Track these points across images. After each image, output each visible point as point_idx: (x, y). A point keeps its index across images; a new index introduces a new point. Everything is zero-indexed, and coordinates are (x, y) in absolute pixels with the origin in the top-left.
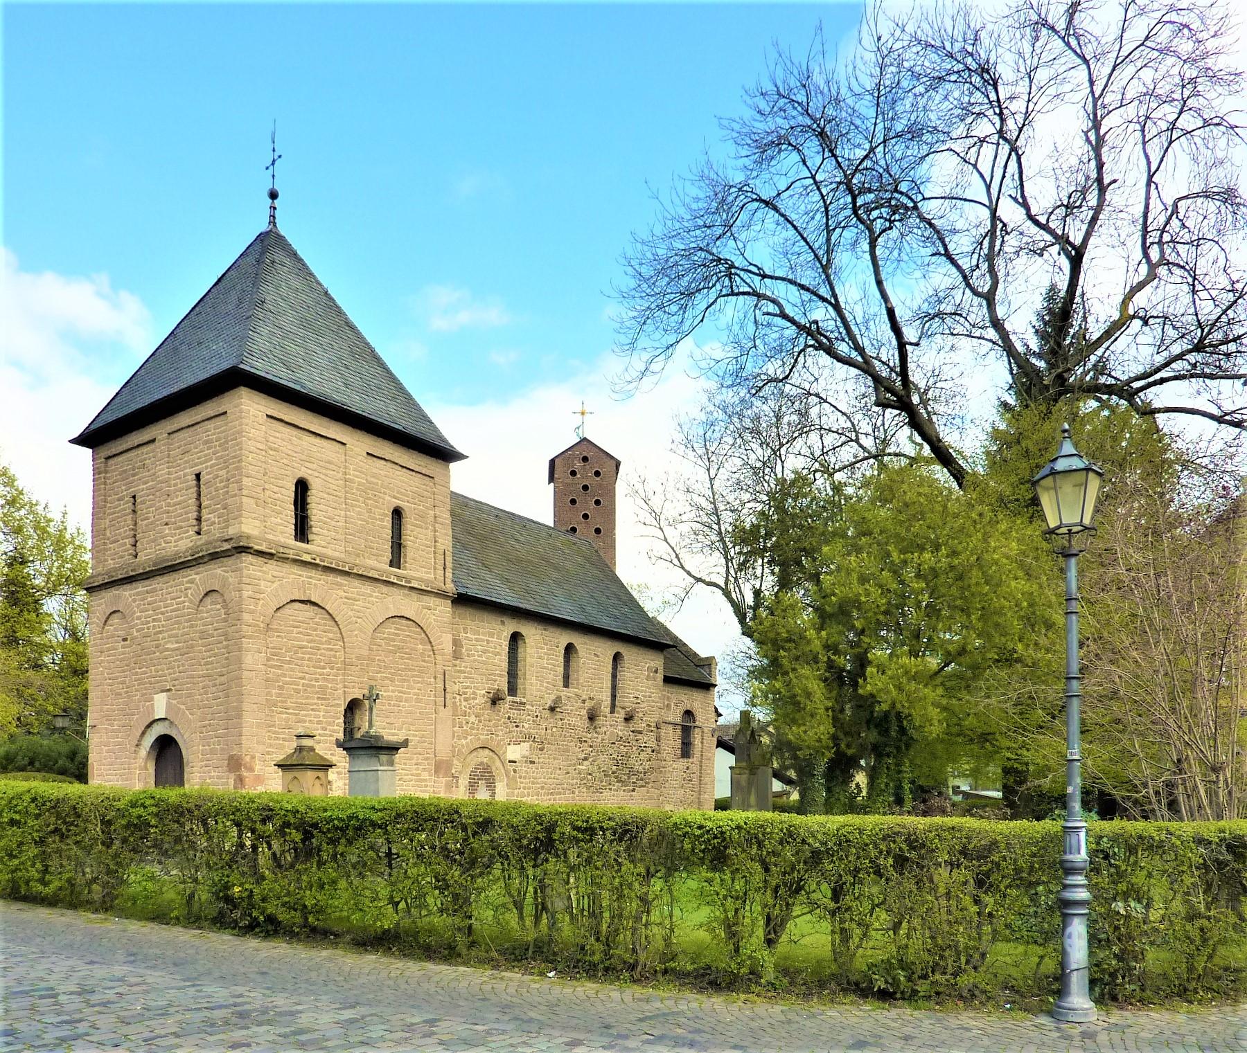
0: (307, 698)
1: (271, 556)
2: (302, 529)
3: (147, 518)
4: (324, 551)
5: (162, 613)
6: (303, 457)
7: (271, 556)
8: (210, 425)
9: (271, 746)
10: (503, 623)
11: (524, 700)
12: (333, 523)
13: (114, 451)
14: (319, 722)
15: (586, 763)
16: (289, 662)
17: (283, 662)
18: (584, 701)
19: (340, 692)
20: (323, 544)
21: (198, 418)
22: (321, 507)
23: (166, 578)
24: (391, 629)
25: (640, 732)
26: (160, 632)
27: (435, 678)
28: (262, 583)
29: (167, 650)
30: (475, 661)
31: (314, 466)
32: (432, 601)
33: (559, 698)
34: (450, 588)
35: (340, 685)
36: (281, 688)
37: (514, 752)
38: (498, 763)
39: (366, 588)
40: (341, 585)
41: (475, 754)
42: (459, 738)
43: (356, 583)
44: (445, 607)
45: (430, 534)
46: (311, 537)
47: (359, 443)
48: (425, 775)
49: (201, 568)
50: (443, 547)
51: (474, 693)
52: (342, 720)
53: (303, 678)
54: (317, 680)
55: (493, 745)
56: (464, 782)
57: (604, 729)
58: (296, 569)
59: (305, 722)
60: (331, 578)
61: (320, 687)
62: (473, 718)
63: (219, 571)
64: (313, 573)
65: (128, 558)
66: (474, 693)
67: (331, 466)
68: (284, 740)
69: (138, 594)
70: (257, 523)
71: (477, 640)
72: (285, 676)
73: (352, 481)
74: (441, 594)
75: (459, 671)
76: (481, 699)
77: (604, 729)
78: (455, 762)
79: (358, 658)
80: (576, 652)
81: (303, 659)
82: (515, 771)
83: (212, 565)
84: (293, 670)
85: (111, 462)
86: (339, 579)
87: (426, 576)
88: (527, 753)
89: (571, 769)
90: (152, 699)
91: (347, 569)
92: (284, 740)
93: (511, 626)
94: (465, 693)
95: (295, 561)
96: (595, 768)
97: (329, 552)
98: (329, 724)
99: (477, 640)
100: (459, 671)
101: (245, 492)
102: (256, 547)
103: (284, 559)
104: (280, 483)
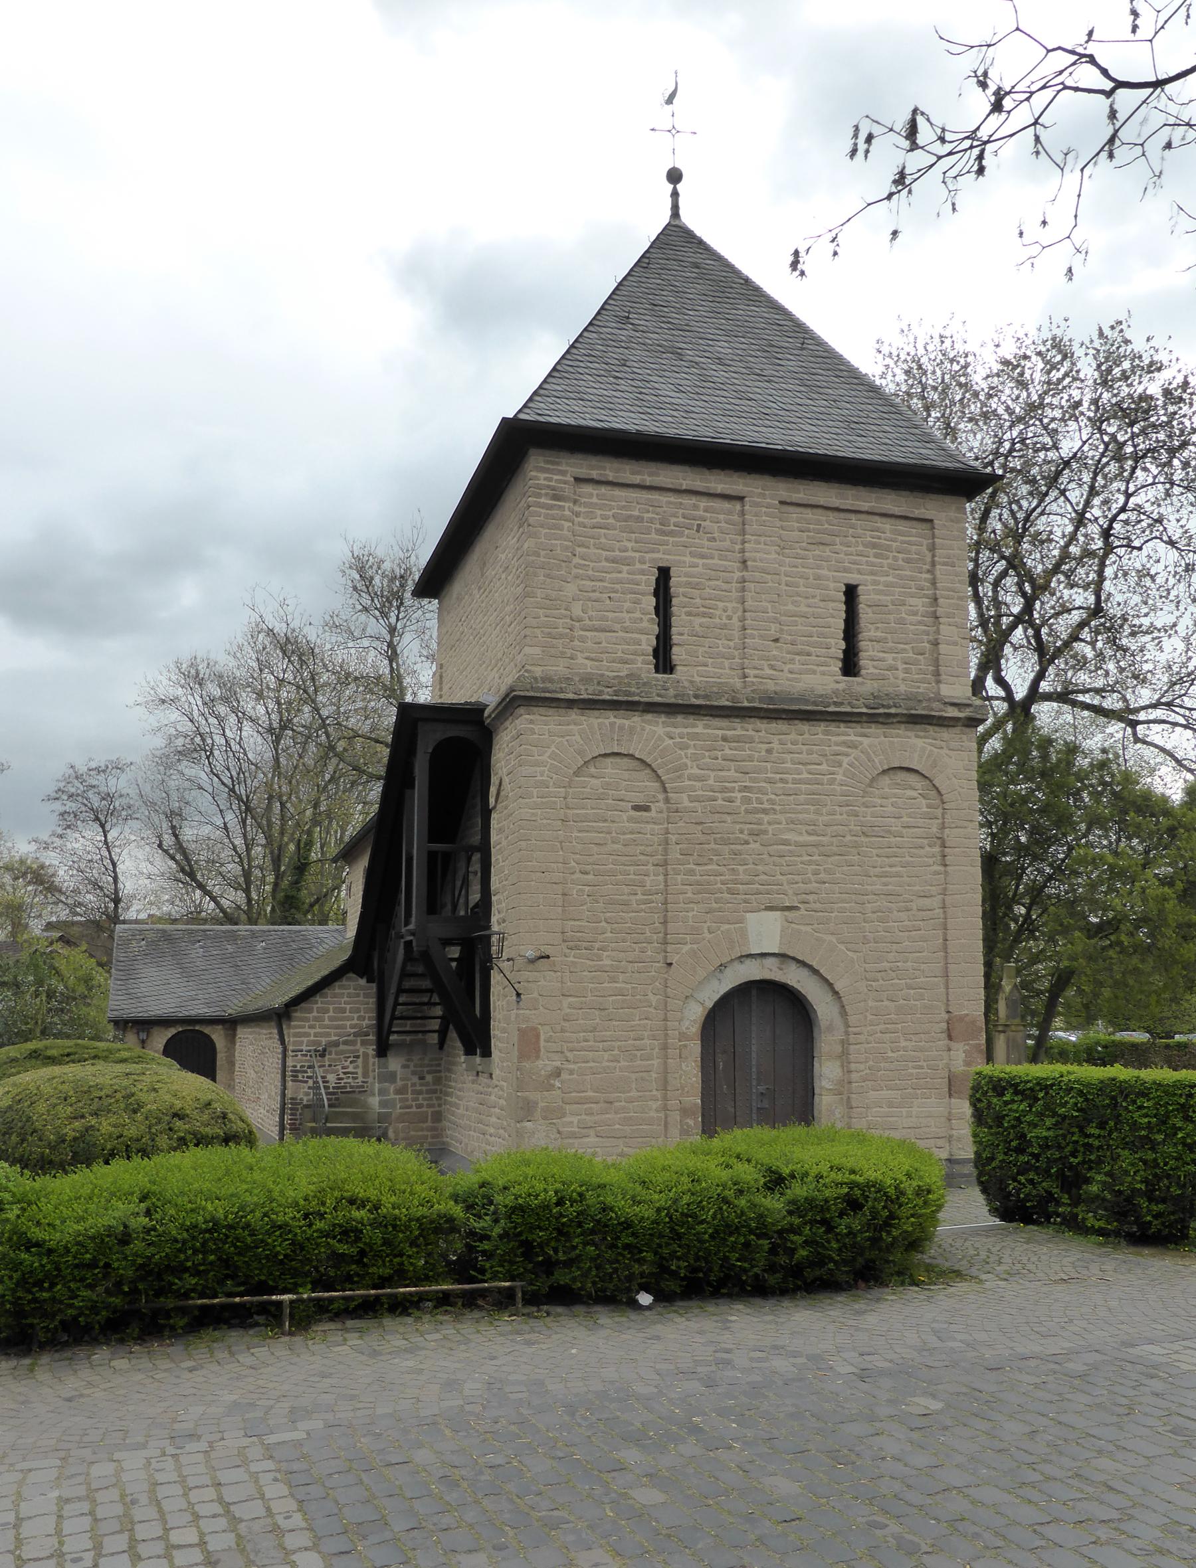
3: (704, 615)
5: (771, 782)
8: (887, 525)
13: (594, 474)
21: (865, 506)
23: (781, 726)
26: (765, 811)
29: (786, 843)
49: (873, 729)
63: (920, 742)
65: (644, 665)
69: (694, 737)
83: (901, 730)
85: (588, 489)
90: (741, 921)
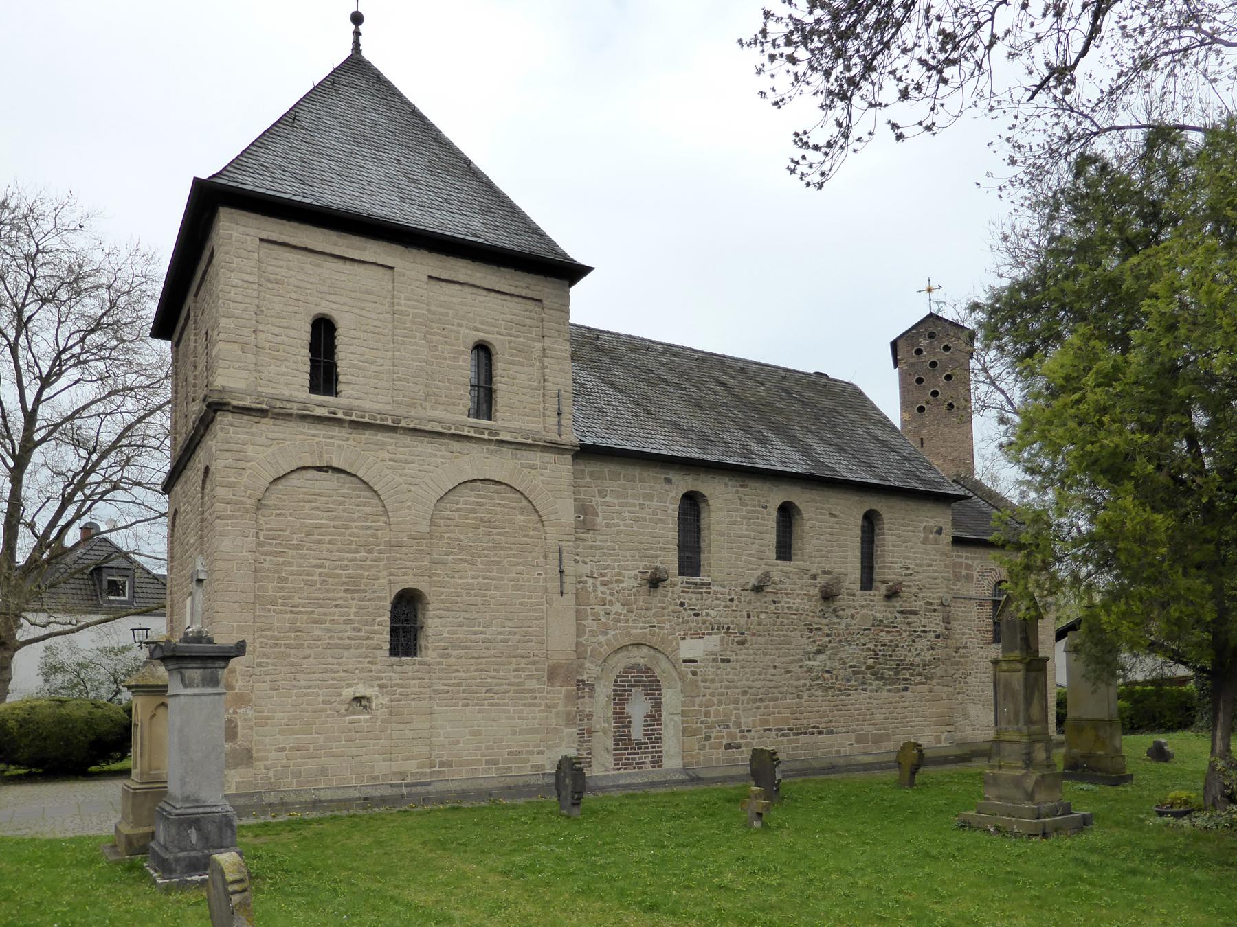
0: (327, 591)
1: (263, 413)
2: (324, 375)
4: (356, 403)
6: (326, 289)
7: (263, 413)
9: (265, 655)
10: (668, 481)
11: (706, 580)
12: (374, 368)
14: (347, 622)
15: (820, 657)
16: (297, 547)
17: (286, 547)
18: (814, 577)
19: (385, 581)
20: (356, 394)
22: (351, 349)
24: (469, 497)
25: (914, 613)
27: (545, 557)
28: (250, 448)
30: (619, 532)
31: (343, 299)
32: (537, 458)
33: (766, 575)
34: (571, 437)
35: (385, 573)
36: (285, 580)
37: (690, 648)
38: (665, 664)
39: (425, 446)
40: (383, 444)
41: (623, 653)
42: (593, 633)
43: (408, 440)
44: (563, 467)
45: (535, 372)
46: (340, 387)
47: (415, 267)
48: (532, 684)
50: (557, 387)
51: (619, 574)
52: (387, 618)
53: (321, 566)
54: (343, 568)
55: (653, 641)
56: (604, 690)
57: (848, 612)
58: (307, 428)
59: (325, 622)
60: (367, 435)
61: (349, 576)
62: (617, 608)
64: (336, 431)
66: (619, 574)
67: (367, 297)
68: (288, 646)
70: (244, 374)
71: (621, 505)
72: (290, 564)
73: (402, 313)
74: (555, 448)
75: (591, 547)
76: (631, 581)
77: (848, 612)
78: (587, 664)
79: (411, 537)
80: (799, 512)
81: (320, 542)
82: (694, 673)
84: (303, 557)
86: (380, 437)
87: (527, 426)
88: (717, 649)
89: (795, 667)
91: (389, 423)
92: (288, 646)
93: (683, 483)
94: (602, 575)
95: (303, 417)
96: (837, 664)
97: (367, 405)
98: (366, 623)
99: (621, 505)
100: (591, 547)
101: (222, 336)
102: (235, 403)
103: (286, 416)
104: (284, 323)
